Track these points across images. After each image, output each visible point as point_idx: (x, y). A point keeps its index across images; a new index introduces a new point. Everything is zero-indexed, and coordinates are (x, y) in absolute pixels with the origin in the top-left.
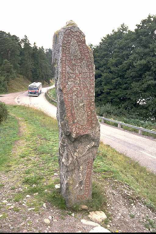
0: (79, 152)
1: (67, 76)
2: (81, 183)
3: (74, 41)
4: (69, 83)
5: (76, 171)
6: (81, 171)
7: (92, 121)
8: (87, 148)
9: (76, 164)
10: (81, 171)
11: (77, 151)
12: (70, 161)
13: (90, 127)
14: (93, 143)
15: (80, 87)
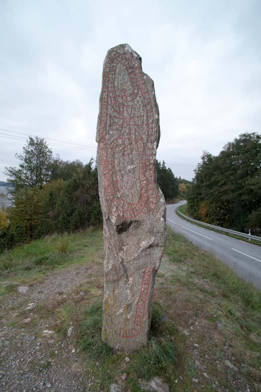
1: (108, 122)
3: (120, 67)
4: (111, 132)
5: (121, 283)
9: (122, 272)
10: (130, 286)
11: (125, 248)
12: (110, 265)
13: (145, 208)
14: (153, 238)
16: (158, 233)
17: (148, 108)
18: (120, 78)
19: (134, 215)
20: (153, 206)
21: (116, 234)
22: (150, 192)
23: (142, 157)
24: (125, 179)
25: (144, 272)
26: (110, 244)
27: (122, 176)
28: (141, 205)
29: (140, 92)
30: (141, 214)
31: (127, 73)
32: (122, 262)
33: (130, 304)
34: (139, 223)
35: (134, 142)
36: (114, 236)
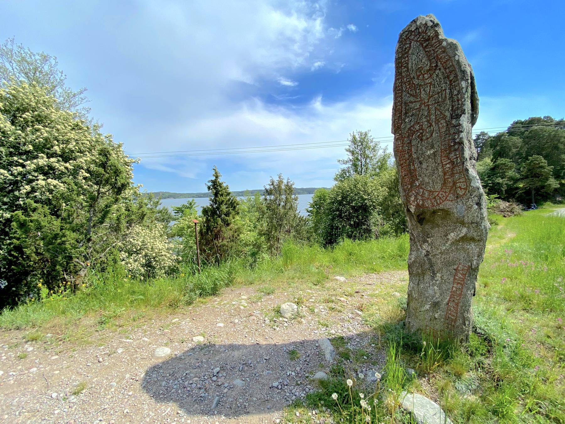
0: (431, 244)
2: (436, 305)
5: (427, 278)
6: (438, 282)
7: (454, 183)
8: (451, 239)
9: (427, 266)
12: (413, 256)
13: (451, 195)
15: (428, 121)
16: (472, 223)
17: (451, 79)
18: (414, 57)
19: (437, 203)
20: (461, 192)
21: (419, 225)
22: (457, 176)
23: (445, 138)
24: (424, 166)
25: (454, 269)
26: (413, 235)
27: (421, 163)
28: (445, 192)
29: (439, 64)
30: (445, 202)
31: (421, 48)
32: (427, 255)
33: (438, 302)
34: (446, 213)
35: (433, 124)
36: (417, 227)
